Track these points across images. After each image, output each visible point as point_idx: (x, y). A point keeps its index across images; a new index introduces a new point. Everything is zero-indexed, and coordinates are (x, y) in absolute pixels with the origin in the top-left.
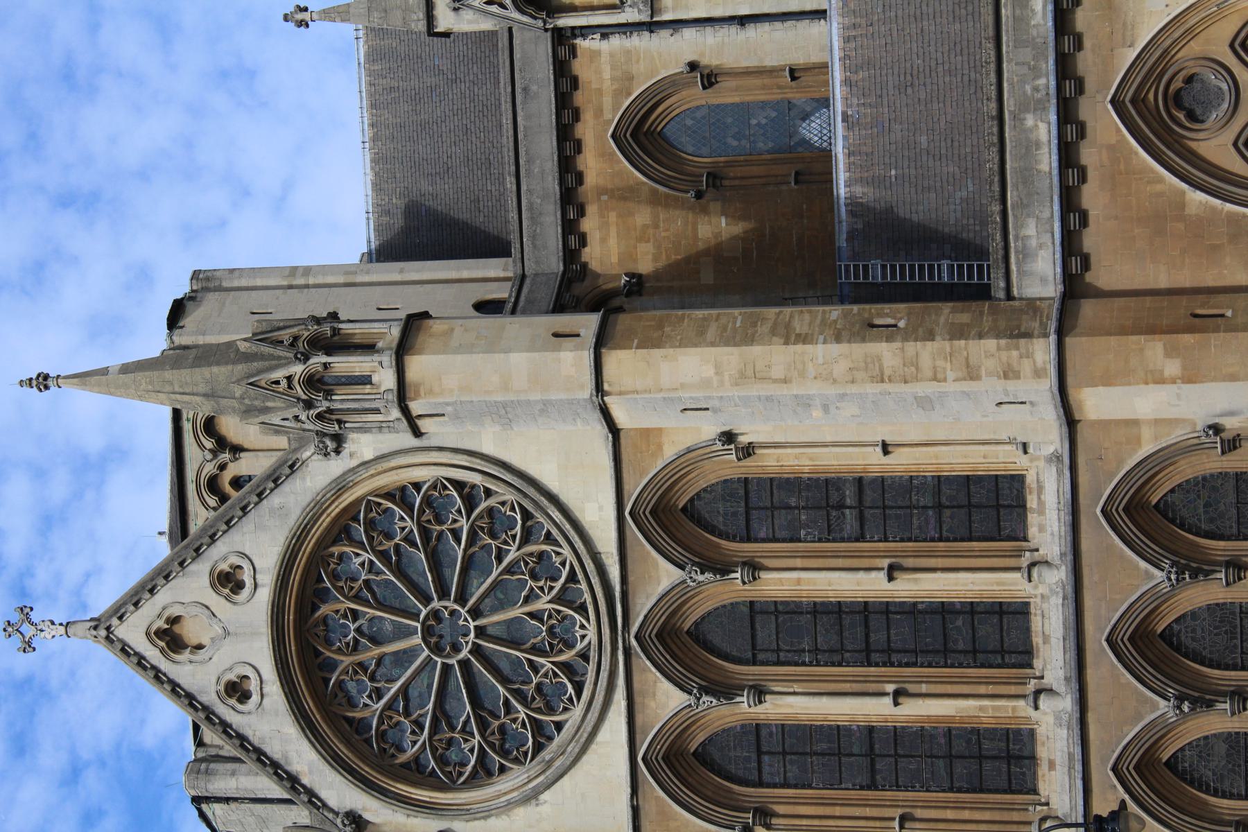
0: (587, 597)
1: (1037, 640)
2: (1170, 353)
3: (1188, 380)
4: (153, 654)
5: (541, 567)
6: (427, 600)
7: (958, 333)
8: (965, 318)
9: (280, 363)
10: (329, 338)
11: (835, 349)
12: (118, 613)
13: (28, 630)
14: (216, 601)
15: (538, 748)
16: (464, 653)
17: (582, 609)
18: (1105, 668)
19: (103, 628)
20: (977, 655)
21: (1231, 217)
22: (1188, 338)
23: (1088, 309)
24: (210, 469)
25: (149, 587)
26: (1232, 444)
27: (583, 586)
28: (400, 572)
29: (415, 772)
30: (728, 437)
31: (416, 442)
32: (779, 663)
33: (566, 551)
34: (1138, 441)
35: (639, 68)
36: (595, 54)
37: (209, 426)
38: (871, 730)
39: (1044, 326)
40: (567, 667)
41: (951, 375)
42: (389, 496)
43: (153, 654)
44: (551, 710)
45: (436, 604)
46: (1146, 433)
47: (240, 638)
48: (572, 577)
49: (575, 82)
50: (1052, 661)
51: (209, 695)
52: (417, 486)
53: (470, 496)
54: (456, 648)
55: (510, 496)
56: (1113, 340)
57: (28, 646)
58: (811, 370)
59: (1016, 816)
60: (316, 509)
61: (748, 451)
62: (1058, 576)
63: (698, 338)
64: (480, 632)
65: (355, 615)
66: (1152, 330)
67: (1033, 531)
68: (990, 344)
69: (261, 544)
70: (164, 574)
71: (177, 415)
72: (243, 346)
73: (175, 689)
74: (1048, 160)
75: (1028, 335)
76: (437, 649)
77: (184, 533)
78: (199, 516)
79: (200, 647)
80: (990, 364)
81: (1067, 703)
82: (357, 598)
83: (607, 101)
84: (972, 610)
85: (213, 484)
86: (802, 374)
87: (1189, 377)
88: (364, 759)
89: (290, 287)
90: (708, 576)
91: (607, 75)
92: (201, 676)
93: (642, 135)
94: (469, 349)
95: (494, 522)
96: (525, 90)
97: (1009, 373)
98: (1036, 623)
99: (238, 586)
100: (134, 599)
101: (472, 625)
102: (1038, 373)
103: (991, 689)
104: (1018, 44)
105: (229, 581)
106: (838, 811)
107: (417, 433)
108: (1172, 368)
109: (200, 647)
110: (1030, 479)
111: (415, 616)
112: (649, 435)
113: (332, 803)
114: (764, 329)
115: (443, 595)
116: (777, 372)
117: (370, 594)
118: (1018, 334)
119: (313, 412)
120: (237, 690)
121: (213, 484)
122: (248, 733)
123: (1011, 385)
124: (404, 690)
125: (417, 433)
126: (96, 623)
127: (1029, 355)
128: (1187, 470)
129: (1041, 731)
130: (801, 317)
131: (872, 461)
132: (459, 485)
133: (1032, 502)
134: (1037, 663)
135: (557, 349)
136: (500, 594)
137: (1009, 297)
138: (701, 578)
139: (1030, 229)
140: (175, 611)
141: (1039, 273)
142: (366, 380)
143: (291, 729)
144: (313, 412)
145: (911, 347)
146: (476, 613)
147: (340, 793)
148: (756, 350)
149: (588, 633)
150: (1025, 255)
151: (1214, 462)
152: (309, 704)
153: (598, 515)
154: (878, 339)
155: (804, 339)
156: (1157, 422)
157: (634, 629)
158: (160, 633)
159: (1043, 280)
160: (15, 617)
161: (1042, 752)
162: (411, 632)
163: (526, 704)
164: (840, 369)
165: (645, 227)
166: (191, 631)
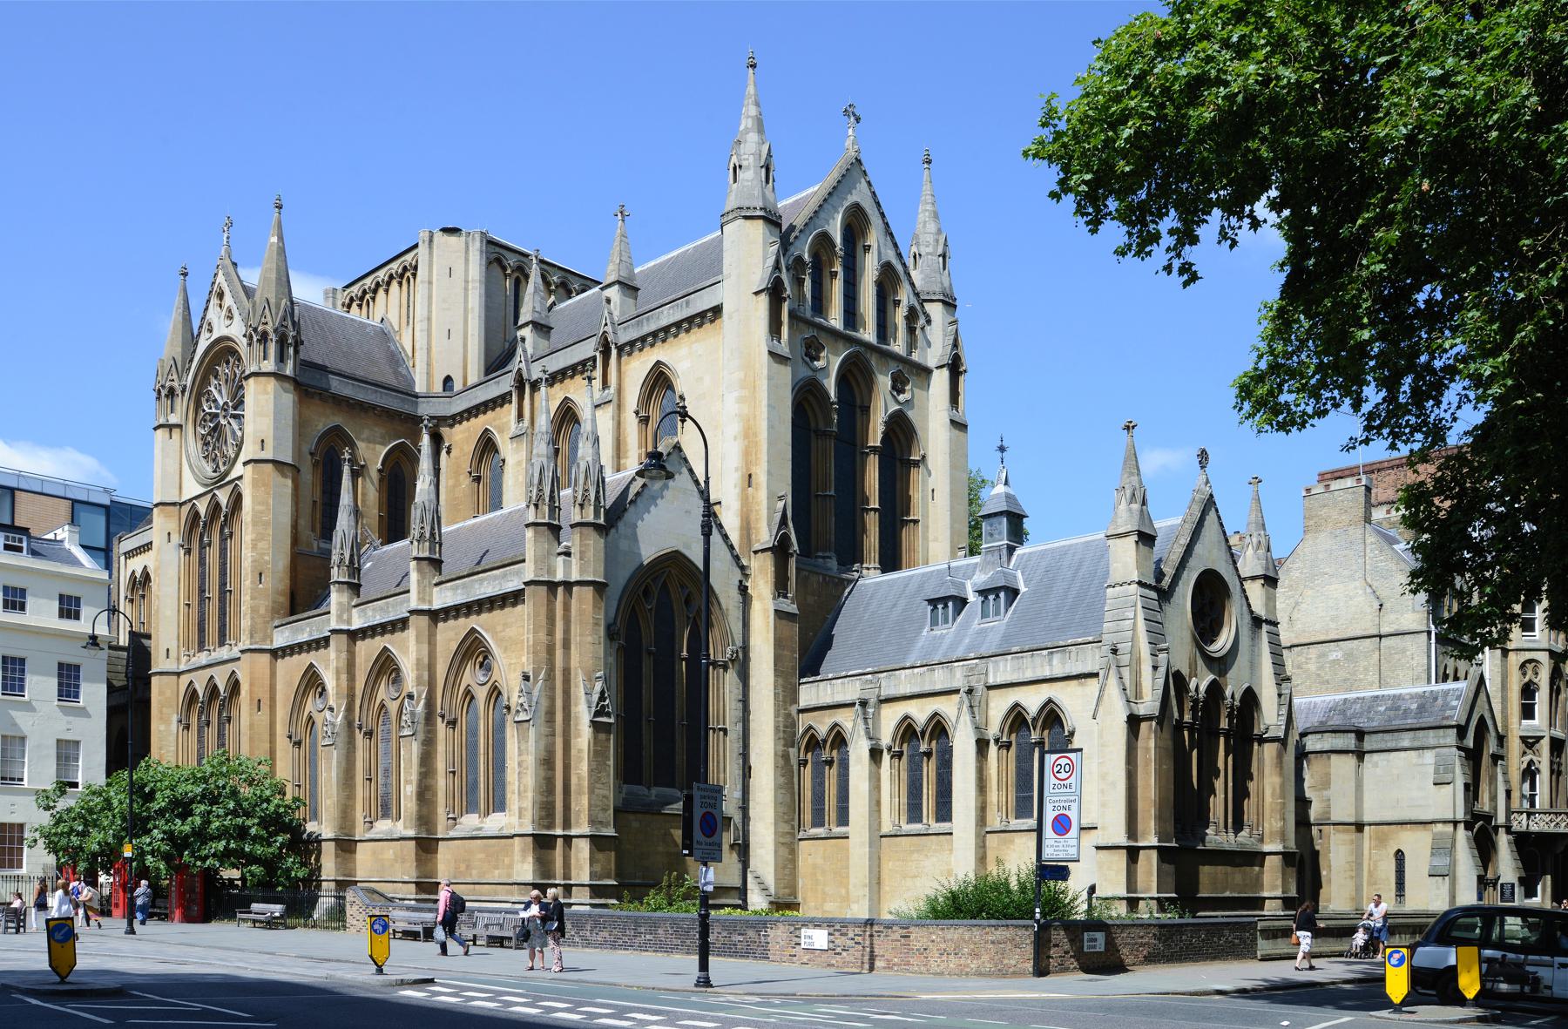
8: (262, 611)
81: (204, 662)
89: (467, 282)
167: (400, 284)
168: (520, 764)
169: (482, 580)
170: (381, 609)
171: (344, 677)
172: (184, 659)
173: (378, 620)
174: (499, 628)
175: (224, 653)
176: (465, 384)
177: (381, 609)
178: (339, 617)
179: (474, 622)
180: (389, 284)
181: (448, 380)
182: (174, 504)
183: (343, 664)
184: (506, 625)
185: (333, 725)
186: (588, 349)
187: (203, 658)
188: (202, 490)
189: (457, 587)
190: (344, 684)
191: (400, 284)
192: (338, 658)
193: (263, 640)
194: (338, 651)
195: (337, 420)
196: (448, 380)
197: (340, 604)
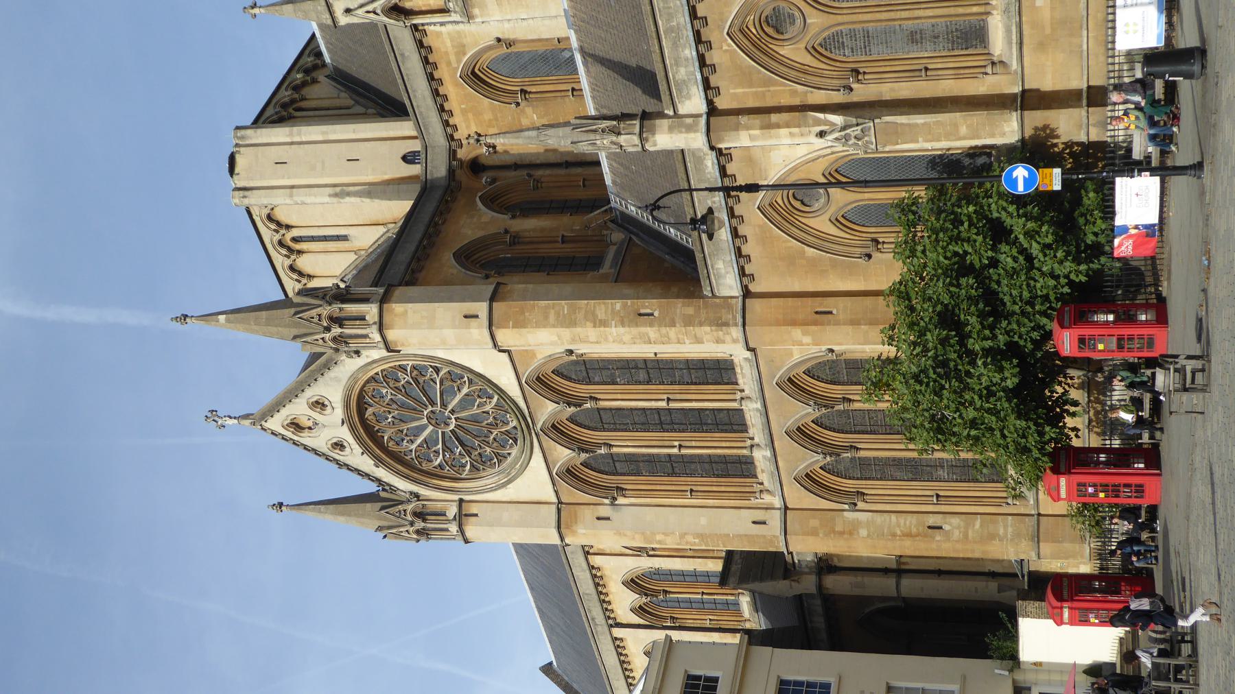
2: (804, 334)
4: (289, 434)
7: (688, 322)
8: (690, 311)
11: (621, 330)
18: (782, 442)
24: (277, 237)
28: (407, 395)
34: (791, 355)
35: (468, 40)
36: (439, 34)
37: (269, 218)
39: (734, 318)
41: (687, 341)
49: (430, 49)
51: (324, 448)
56: (774, 328)
58: (611, 339)
59: (747, 489)
63: (543, 323)
66: (794, 323)
68: (708, 329)
75: (726, 324)
76: (437, 425)
80: (708, 337)
83: (453, 58)
85: (281, 243)
89: (292, 143)
91: (449, 44)
93: (475, 78)
96: (402, 55)
102: (735, 341)
106: (658, 487)
114: (580, 315)
116: (593, 339)
118: (722, 324)
121: (281, 243)
135: (468, 327)
137: (714, 296)
139: (720, 265)
141: (727, 283)
142: (366, 336)
145: (664, 330)
148: (579, 330)
150: (718, 276)
154: (645, 325)
155: (604, 323)
159: (731, 287)
164: (627, 338)
165: (490, 120)
167: (300, 252)
170: (675, 45)
171: (774, 118)
172: (767, 499)
173: (690, 52)
175: (746, 379)
176: (415, 138)
177: (675, 45)
178: (690, 129)
180: (301, 274)
181: (408, 158)
182: (559, 510)
183: (756, 120)
185: (844, 128)
187: (761, 457)
188: (537, 459)
190: (785, 116)
191: (300, 252)
192: (748, 128)
193: (730, 308)
194: (737, 128)
195: (447, 258)
196: (408, 158)
197: (671, 129)
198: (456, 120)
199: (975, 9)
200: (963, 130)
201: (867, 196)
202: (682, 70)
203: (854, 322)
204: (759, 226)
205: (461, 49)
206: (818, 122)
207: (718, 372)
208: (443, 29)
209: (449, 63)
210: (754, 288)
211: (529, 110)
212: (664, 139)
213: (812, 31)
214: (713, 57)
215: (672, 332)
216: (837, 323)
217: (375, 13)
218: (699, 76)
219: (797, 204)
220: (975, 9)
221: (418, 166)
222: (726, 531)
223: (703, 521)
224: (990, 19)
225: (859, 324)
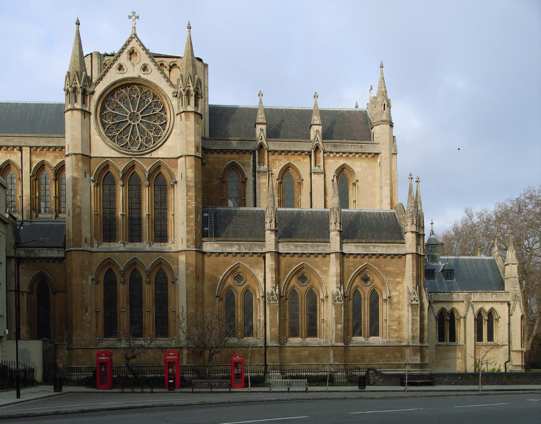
0: (142, 150)
1: (134, 244)
3: (187, 275)
5: (148, 141)
6: (141, 114)
7: (196, 232)
9: (193, 86)
10: (198, 96)
12: (138, 40)
13: (134, 17)
14: (141, 64)
15: (109, 137)
16: (129, 122)
17: (139, 149)
19: (134, 36)
20: (131, 230)
21: (217, 284)
22: (194, 276)
23: (200, 256)
25: (144, 49)
26: (173, 283)
27: (144, 149)
29: (103, 109)
30: (176, 182)
31: (175, 114)
32: (129, 190)
33: (151, 146)
34: (174, 265)
38: (115, 209)
40: (127, 143)
42: (163, 107)
43: (129, 48)
44: (118, 140)
45: (140, 116)
46: (175, 267)
47: (132, 71)
48: (146, 147)
50: (131, 246)
52: (165, 114)
53: (164, 125)
54: (130, 120)
55: (164, 134)
57: (130, 17)
60: (161, 90)
61: (173, 186)
62: (148, 248)
64: (134, 125)
65: (138, 97)
67: (156, 244)
69: (154, 77)
70: (147, 52)
71: (179, 57)
72: (196, 76)
73: (120, 53)
74: (229, 250)
77: (154, 57)
78: (157, 60)
79: (130, 59)
80: (190, 237)
82: (141, 98)
84: (140, 230)
86: (189, 199)
87: (187, 275)
88: (106, 97)
90: (147, 176)
92: (124, 59)
94: (195, 128)
95: (157, 131)
97: (188, 241)
98: (138, 244)
99: (144, 70)
100: (141, 45)
101: (136, 124)
102: (188, 247)
103: (124, 234)
104: (251, 245)
105: (145, 68)
107: (177, 115)
108: (189, 272)
109: (130, 59)
110: (166, 244)
111: (138, 111)
112: (176, 166)
113: (96, 88)
115: (142, 118)
117: (142, 101)
119: (182, 91)
120: (120, 68)
122: (111, 69)
123: (186, 241)
124: (120, 107)
125: (177, 115)
126: (135, 35)
127: (192, 245)
128: (169, 275)
129: (116, 244)
130: (200, 200)
131: (170, 213)
132: (166, 123)
133: (162, 244)
134: (130, 243)
136: (142, 132)
138: (147, 175)
139: (216, 246)
140: (138, 55)
143: (113, 80)
144: (182, 91)
145: (194, 221)
146: (138, 124)
147: (99, 89)
149: (135, 149)
151: (170, 279)
152: (118, 85)
153: (160, 153)
156: (178, 269)
157: (135, 159)
158: (133, 51)
160: (136, 15)
161: (112, 243)
162: (134, 110)
163: (119, 134)
166: (134, 58)
168: (412, 320)
169: (374, 246)
170: (301, 246)
174: (382, 266)
179: (366, 261)
184: (386, 266)
186: (307, 147)
189: (358, 246)
198: (216, 155)
199: (304, 334)
200: (274, 329)
201: (239, 298)
202: (293, 247)
203: (196, 289)
204: (231, 262)
205: (243, 164)
206: (276, 286)
207: (161, 235)
208: (251, 161)
209: (239, 159)
210: (206, 256)
211: (218, 182)
212: (270, 237)
213: (300, 288)
214: (296, 257)
215: (193, 224)
216: (196, 283)
217: (261, 139)
218: (291, 252)
219: (236, 275)
220: (304, 334)
221: (208, 137)
222: (83, 226)
223: (86, 217)
224: (299, 339)
225: (196, 291)
